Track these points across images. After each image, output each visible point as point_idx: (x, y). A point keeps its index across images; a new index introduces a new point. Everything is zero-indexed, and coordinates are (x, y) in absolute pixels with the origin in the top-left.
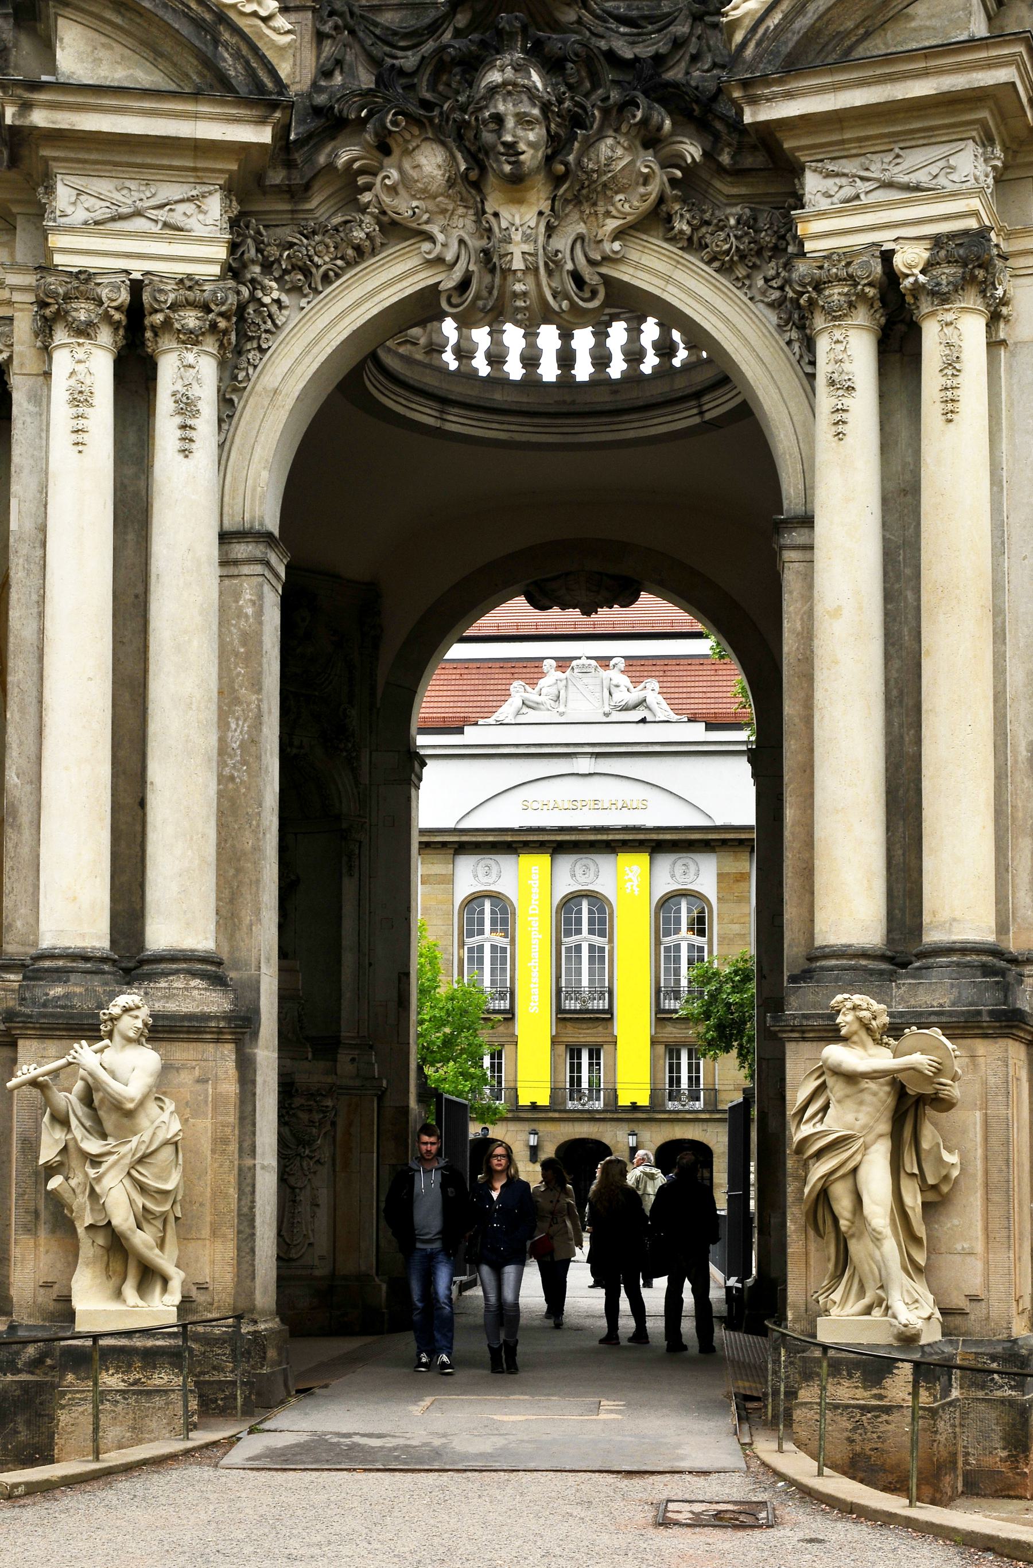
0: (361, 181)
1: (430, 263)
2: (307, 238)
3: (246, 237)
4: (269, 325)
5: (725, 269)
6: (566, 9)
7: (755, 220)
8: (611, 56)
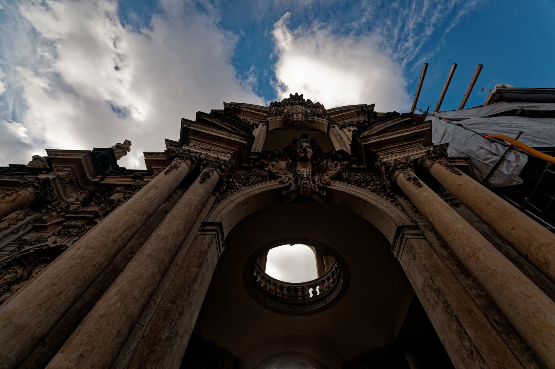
5: (359, 186)
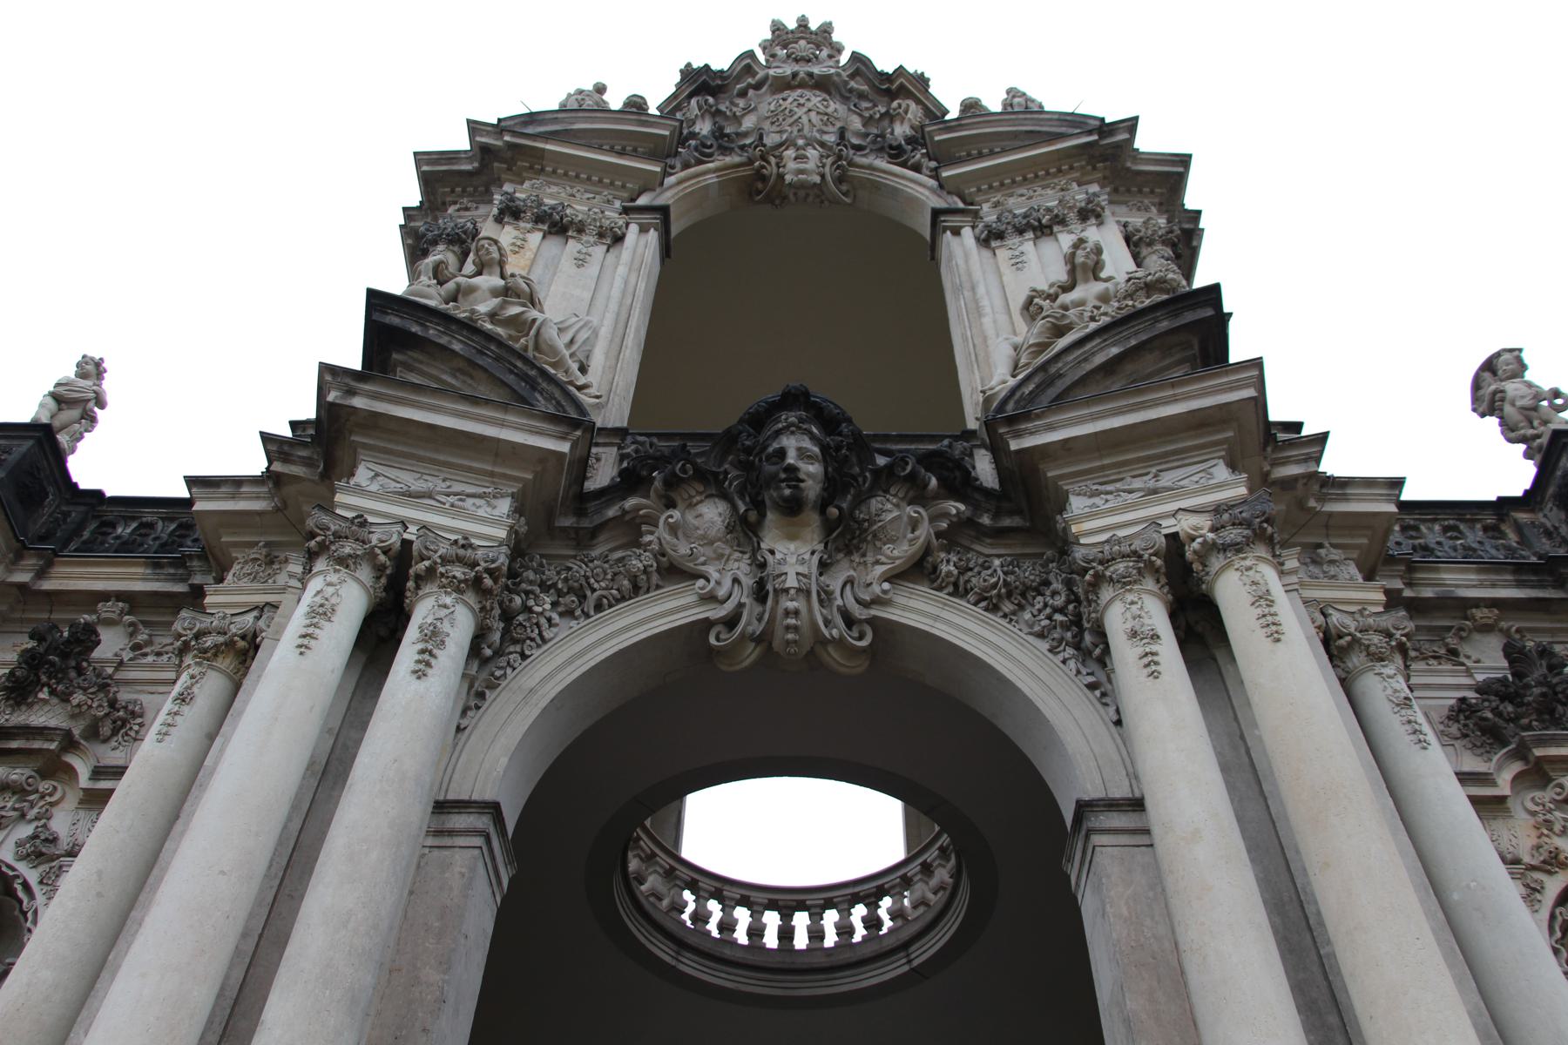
4: (535, 634)
5: (993, 608)
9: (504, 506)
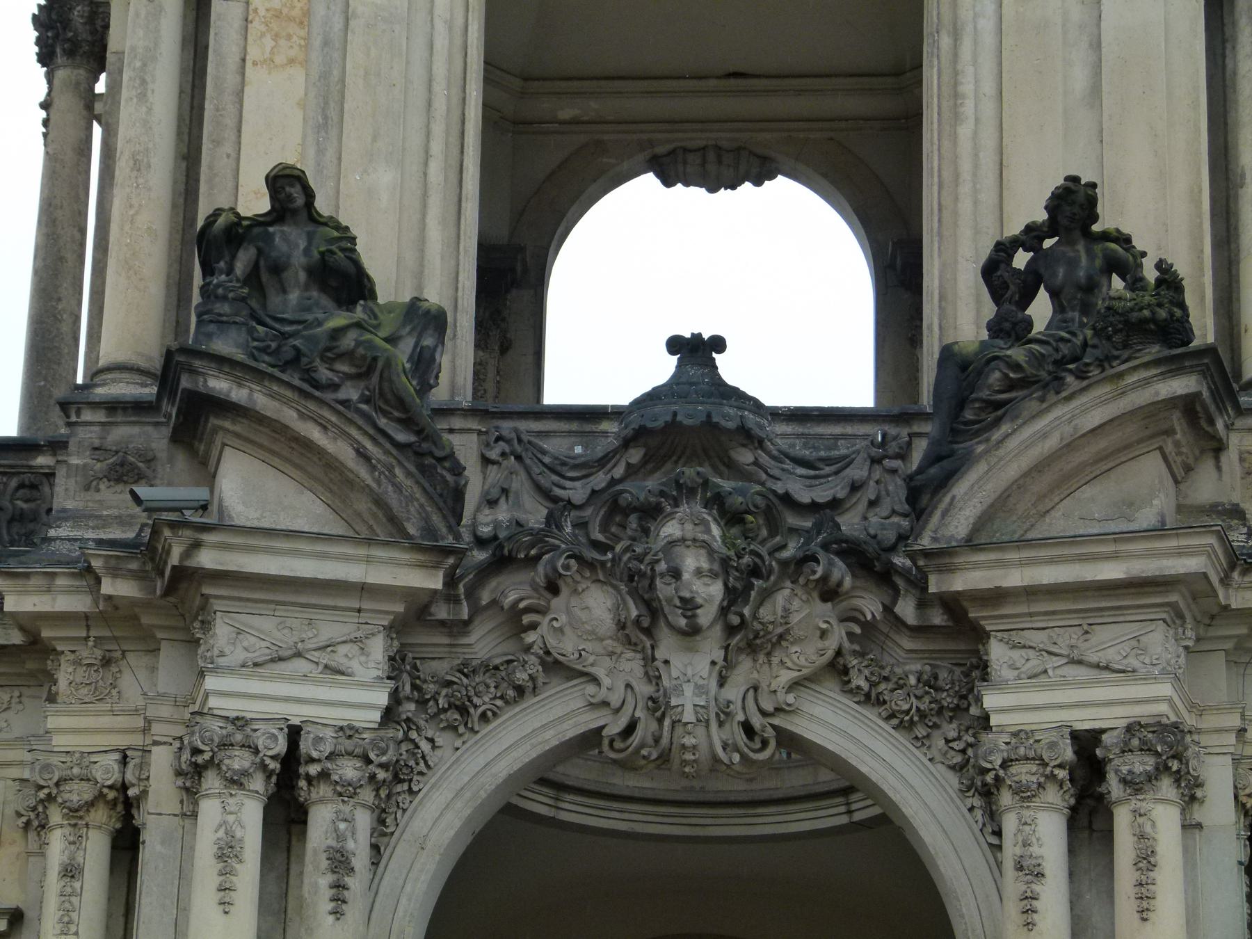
0: (526, 619)
1: (592, 706)
2: (466, 676)
3: (401, 671)
4: (422, 766)
5: (905, 726)
6: (743, 450)
7: (936, 678)
8: (787, 499)
9: (378, 649)
